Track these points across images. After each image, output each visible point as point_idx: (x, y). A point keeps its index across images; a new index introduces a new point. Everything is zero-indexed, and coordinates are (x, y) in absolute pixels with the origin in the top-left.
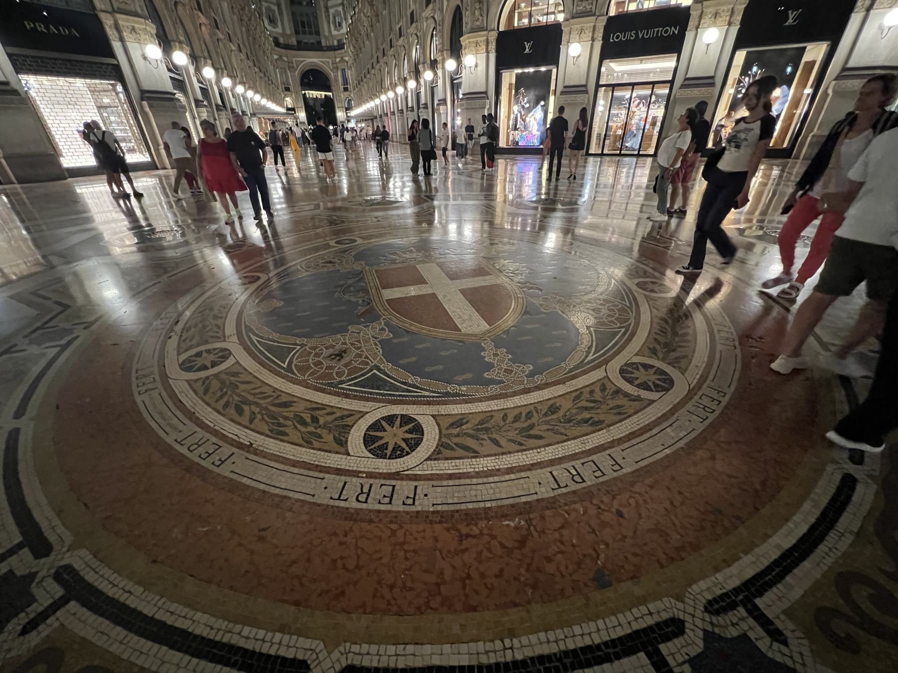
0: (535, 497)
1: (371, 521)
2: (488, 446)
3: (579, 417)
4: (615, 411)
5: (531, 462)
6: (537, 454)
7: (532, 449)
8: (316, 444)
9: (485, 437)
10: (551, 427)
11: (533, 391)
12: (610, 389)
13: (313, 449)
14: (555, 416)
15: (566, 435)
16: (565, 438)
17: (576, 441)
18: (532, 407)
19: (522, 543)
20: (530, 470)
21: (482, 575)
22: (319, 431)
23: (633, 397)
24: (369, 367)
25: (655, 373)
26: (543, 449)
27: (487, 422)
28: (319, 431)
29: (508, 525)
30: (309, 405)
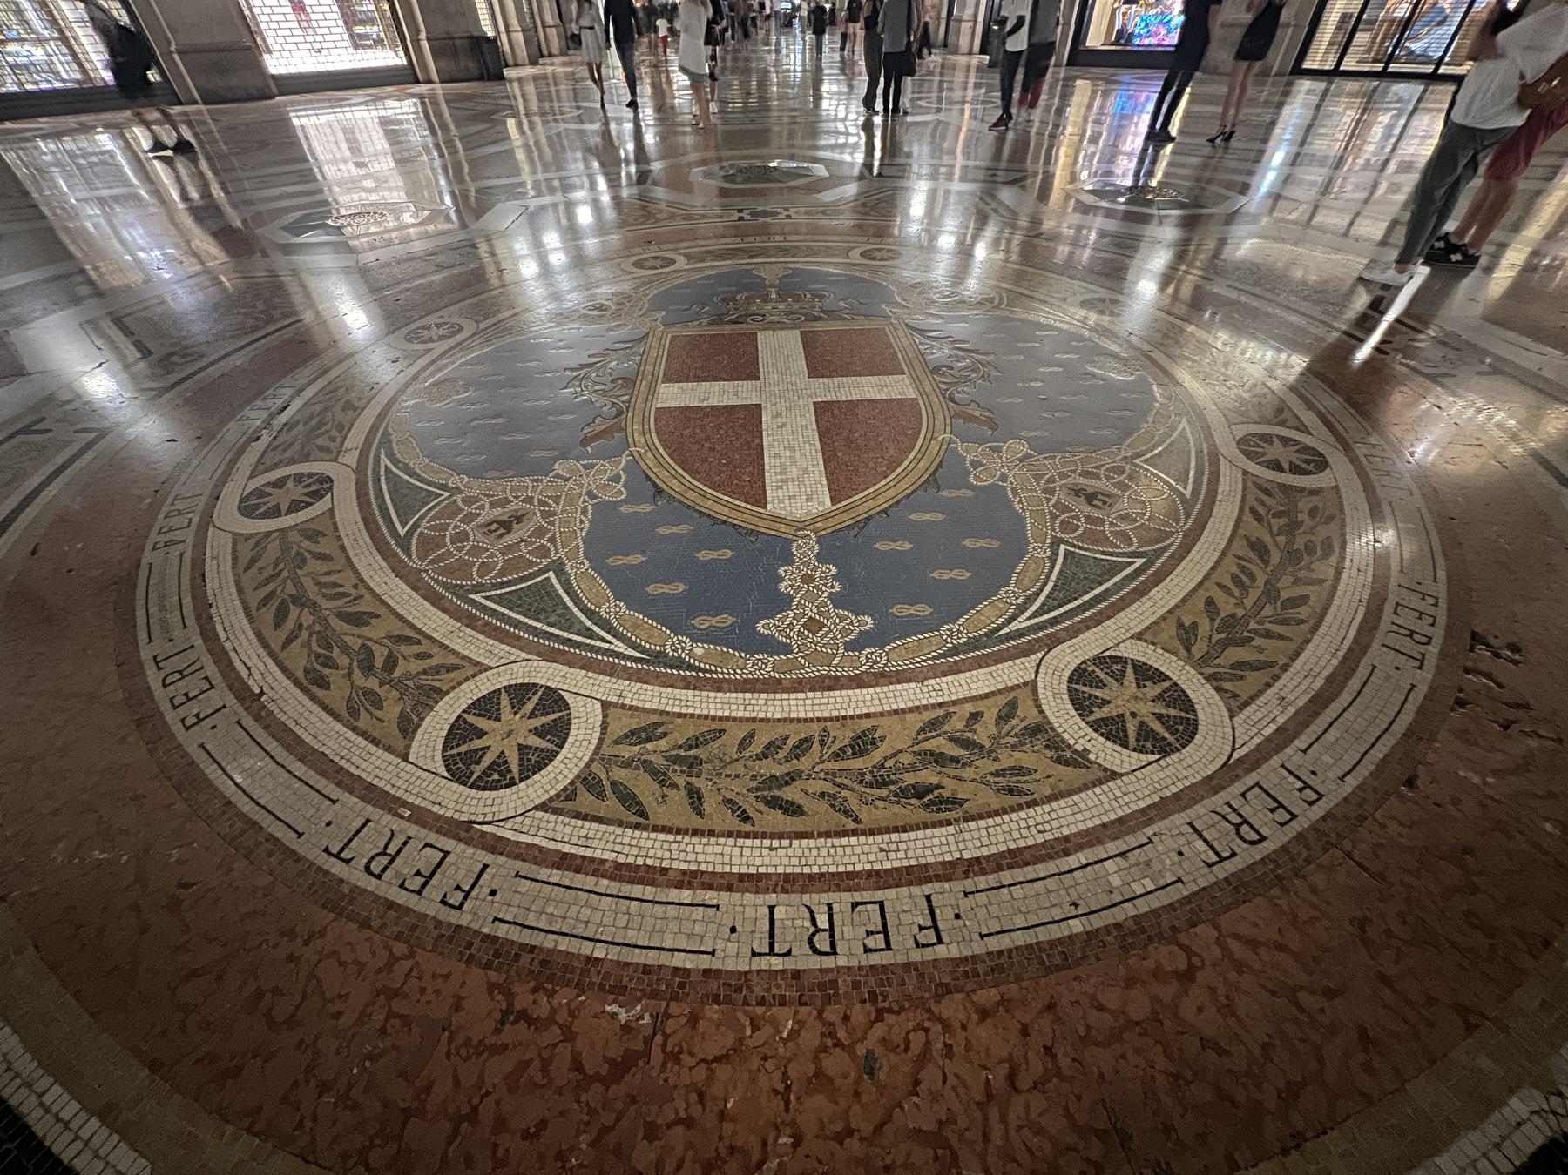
0: (705, 962)
1: (365, 924)
3: (910, 779)
4: (1003, 781)
5: (744, 870)
6: (766, 852)
7: (764, 836)
11: (842, 688)
12: (1027, 714)
14: (858, 763)
15: (856, 820)
16: (851, 825)
17: (870, 840)
18: (816, 729)
19: (621, 1067)
20: (730, 888)
21: (500, 1124)
23: (1068, 754)
26: (785, 842)
27: (706, 742)
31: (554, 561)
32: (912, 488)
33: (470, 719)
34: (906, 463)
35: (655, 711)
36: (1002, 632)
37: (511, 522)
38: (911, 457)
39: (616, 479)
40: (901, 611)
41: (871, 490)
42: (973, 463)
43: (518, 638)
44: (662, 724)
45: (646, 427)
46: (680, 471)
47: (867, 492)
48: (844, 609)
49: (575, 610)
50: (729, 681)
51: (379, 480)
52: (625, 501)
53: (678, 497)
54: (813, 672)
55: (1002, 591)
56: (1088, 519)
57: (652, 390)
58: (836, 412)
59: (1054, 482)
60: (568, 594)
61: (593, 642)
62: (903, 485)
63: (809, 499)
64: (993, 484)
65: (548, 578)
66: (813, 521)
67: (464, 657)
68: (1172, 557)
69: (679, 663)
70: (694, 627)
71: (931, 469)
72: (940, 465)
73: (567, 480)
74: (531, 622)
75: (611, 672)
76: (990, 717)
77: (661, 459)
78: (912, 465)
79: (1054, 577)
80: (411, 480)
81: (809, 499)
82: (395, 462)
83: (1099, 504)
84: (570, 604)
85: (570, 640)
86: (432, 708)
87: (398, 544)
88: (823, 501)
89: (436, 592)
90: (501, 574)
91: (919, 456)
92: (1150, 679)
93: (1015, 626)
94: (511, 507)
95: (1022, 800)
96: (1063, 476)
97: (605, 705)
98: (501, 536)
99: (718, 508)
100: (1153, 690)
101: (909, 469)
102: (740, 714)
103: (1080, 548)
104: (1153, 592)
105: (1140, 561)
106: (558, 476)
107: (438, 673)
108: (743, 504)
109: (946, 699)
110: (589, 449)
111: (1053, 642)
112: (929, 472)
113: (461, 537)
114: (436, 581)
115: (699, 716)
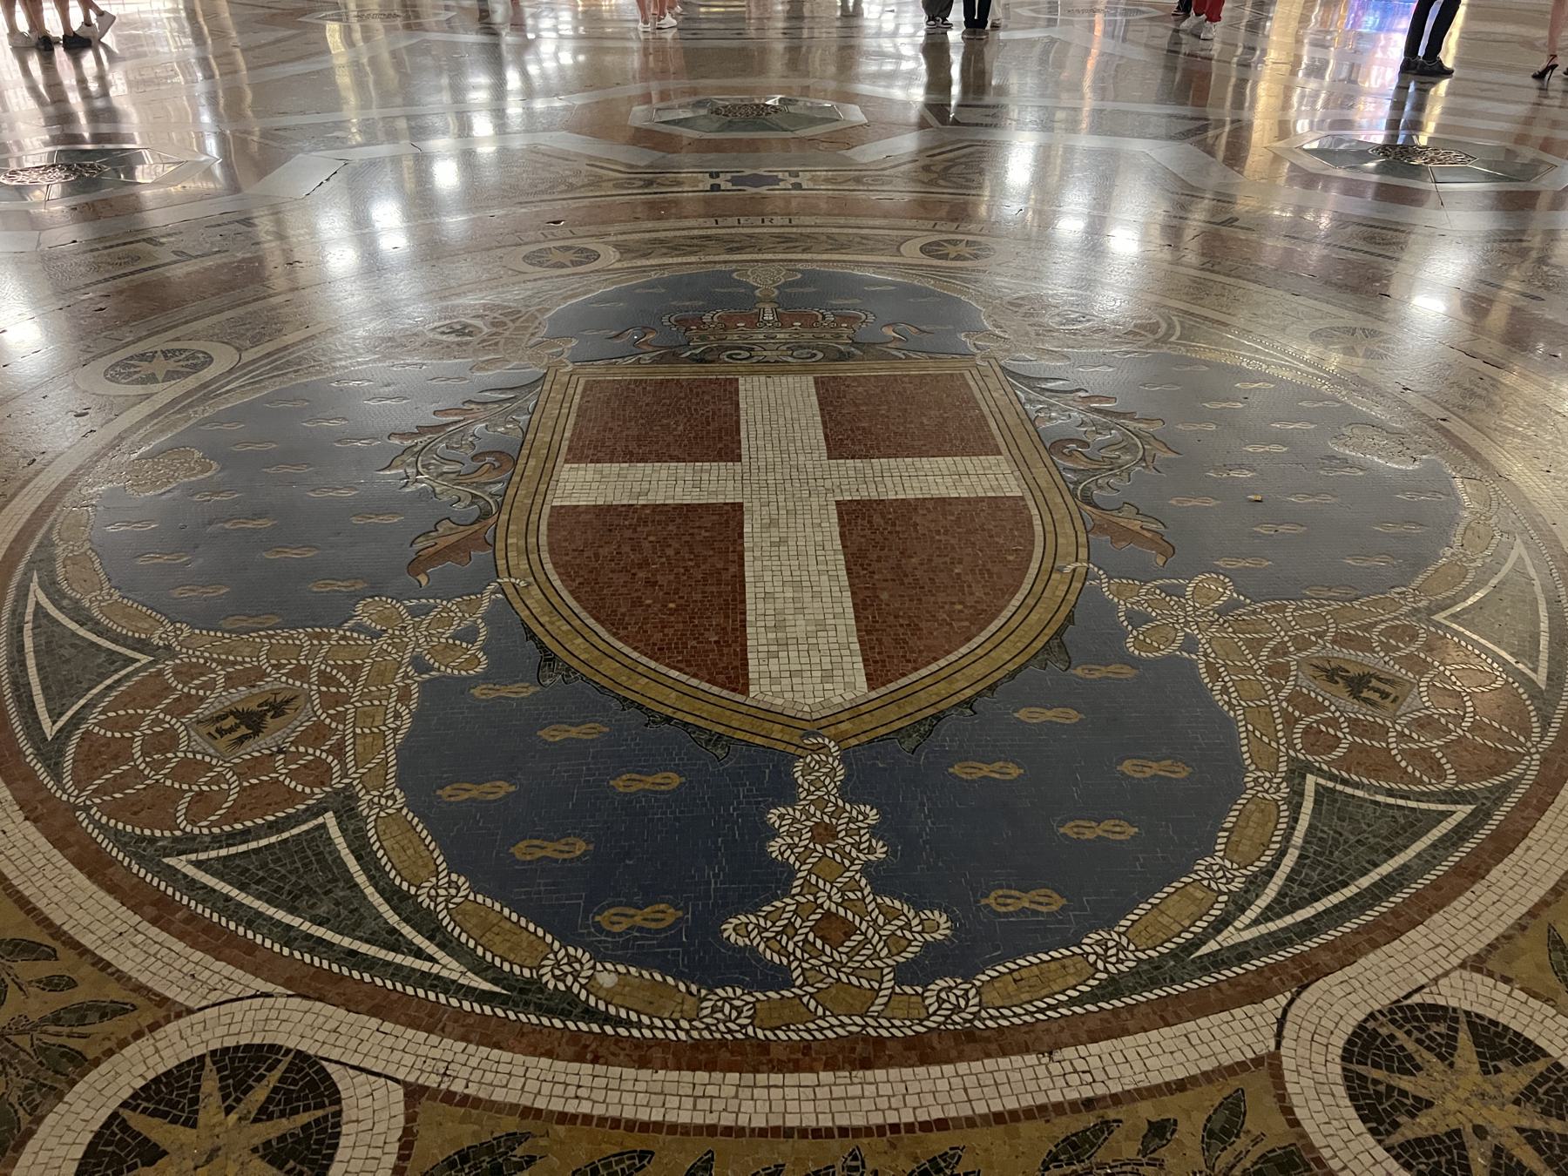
12: (1262, 1121)
25: (1529, 1094)
31: (337, 792)
32: (1020, 660)
33: (137, 1121)
34: (1007, 613)
35: (513, 1108)
36: (1204, 950)
37: (262, 715)
38: (1015, 602)
39: (469, 635)
40: (1005, 902)
41: (942, 663)
42: (1130, 616)
43: (251, 947)
44: (526, 1136)
45: (531, 540)
46: (591, 622)
47: (934, 667)
48: (893, 896)
49: (369, 891)
50: (665, 1044)
51: (20, 630)
52: (485, 677)
53: (584, 670)
54: (833, 1027)
55: (1200, 866)
56: (1354, 724)
57: (547, 473)
58: (877, 519)
59: (1286, 653)
60: (358, 858)
61: (399, 959)
62: (1003, 654)
63: (827, 676)
64: (1170, 657)
65: (323, 826)
66: (833, 719)
67: (140, 988)
68: (1523, 803)
69: (567, 1006)
70: (599, 929)
71: (1054, 627)
72: (1070, 618)
73: (376, 635)
74: (280, 915)
75: (430, 1021)
76: (1190, 1132)
77: (555, 600)
78: (1018, 618)
79: (1298, 838)
80: (82, 632)
81: (827, 676)
82: (56, 596)
83: (1375, 696)
84: (361, 879)
85: (353, 953)
86: (60, 1097)
87: (39, 754)
88: (852, 683)
89: (100, 850)
90: (233, 815)
91: (1030, 601)
92: (1507, 1054)
93: (1230, 937)
94: (266, 685)
96: (1302, 643)
97: (414, 1093)
98: (241, 740)
99: (656, 691)
100: (1514, 1079)
101: (1013, 624)
102: (684, 1118)
103: (1345, 782)
104: (1495, 874)
105: (1463, 811)
106: (359, 628)
107: (81, 1021)
108: (705, 686)
109: (1100, 1090)
110: (423, 579)
111: (1306, 974)
112: (1049, 632)
113: (164, 742)
114: (103, 828)
115: (602, 1120)
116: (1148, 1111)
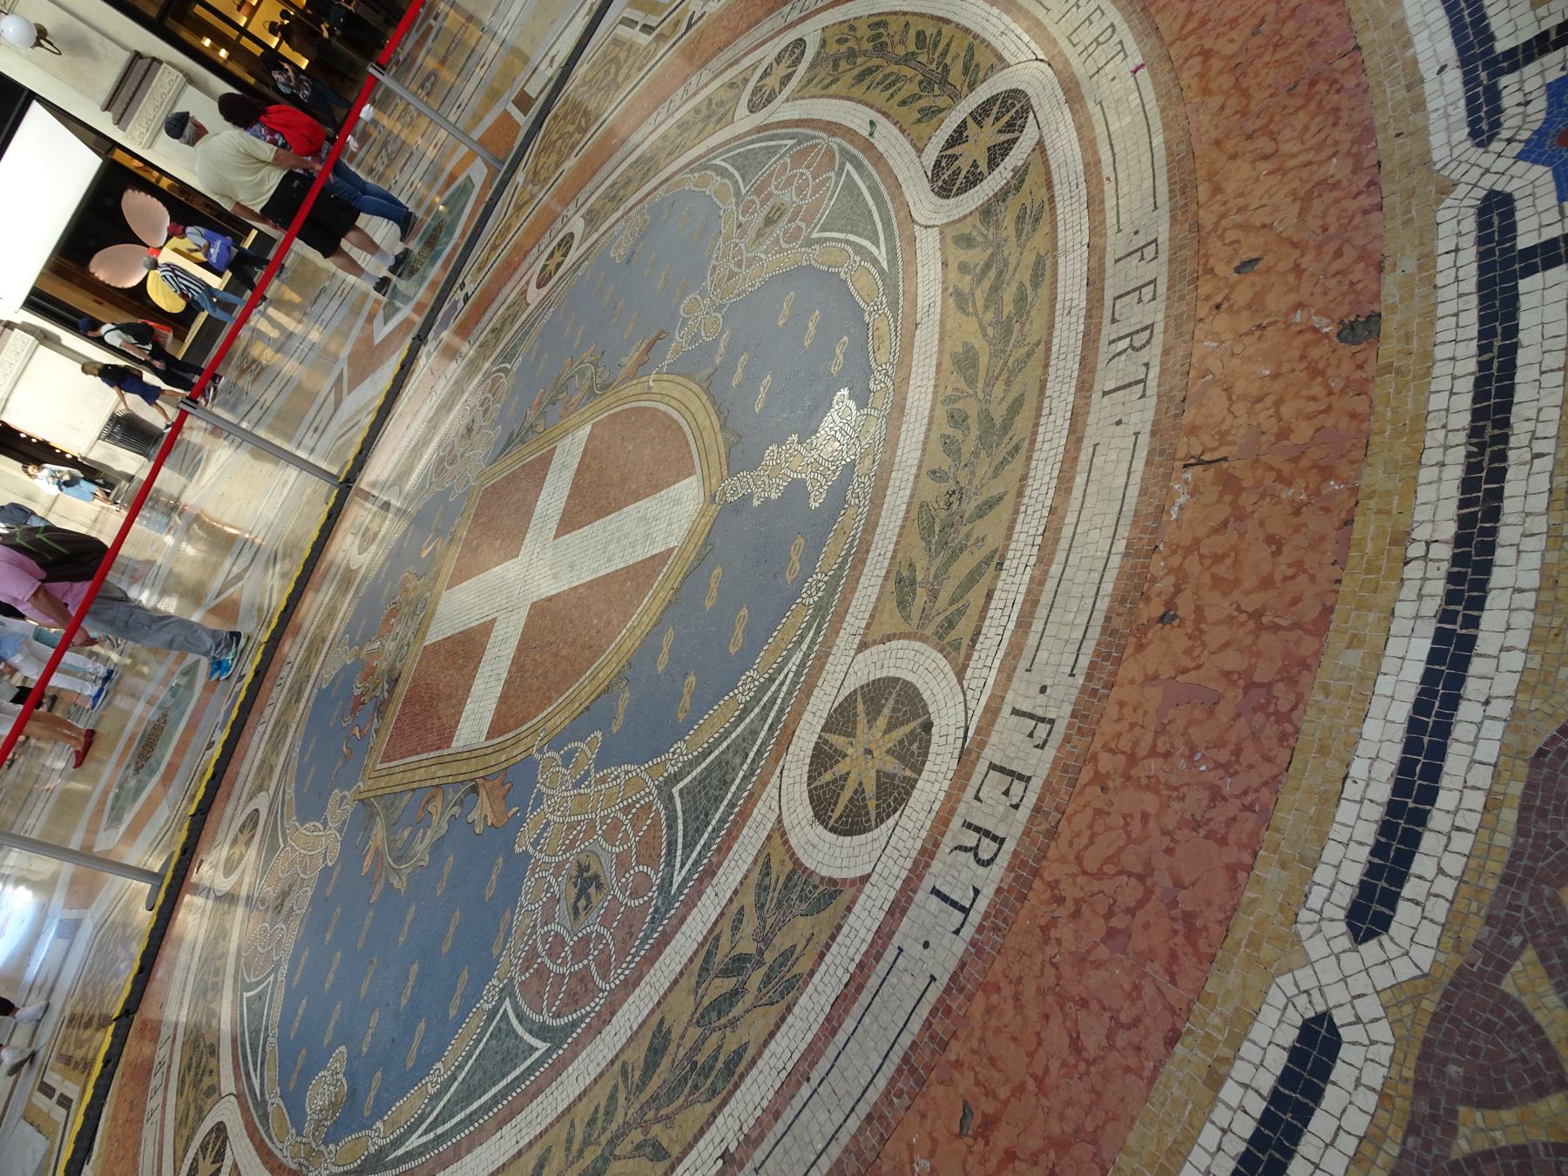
0: (1144, 439)
2: (990, 528)
3: (1008, 308)
5: (1065, 433)
6: (1052, 418)
7: (1037, 425)
8: (803, 966)
9: (964, 530)
10: (1004, 377)
13: (812, 973)
15: (1037, 345)
16: (1042, 347)
17: (1058, 326)
20: (1080, 440)
21: (1266, 583)
22: (769, 957)
24: (659, 805)
25: (979, 124)
26: (1046, 402)
28: (769, 957)
29: (1181, 508)
30: (689, 981)
76: (963, 255)
95: (1047, 207)
116: (954, 275)
